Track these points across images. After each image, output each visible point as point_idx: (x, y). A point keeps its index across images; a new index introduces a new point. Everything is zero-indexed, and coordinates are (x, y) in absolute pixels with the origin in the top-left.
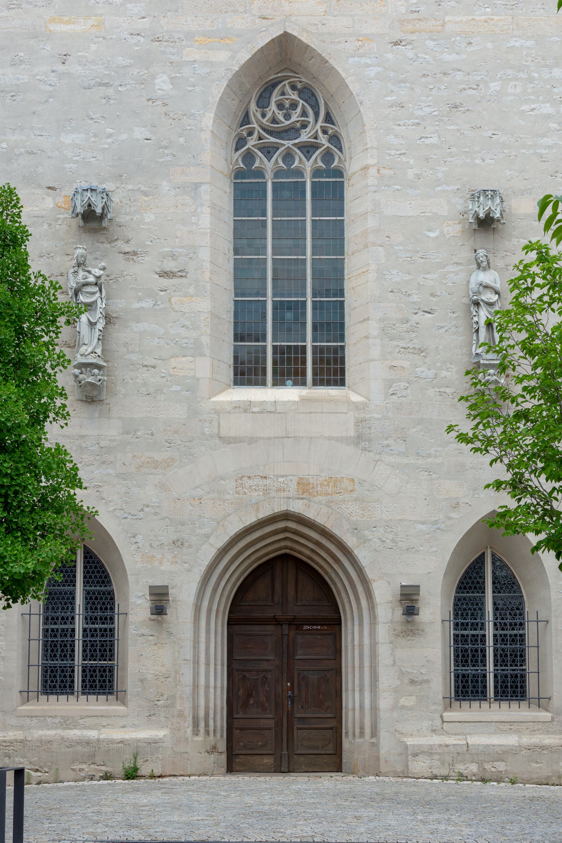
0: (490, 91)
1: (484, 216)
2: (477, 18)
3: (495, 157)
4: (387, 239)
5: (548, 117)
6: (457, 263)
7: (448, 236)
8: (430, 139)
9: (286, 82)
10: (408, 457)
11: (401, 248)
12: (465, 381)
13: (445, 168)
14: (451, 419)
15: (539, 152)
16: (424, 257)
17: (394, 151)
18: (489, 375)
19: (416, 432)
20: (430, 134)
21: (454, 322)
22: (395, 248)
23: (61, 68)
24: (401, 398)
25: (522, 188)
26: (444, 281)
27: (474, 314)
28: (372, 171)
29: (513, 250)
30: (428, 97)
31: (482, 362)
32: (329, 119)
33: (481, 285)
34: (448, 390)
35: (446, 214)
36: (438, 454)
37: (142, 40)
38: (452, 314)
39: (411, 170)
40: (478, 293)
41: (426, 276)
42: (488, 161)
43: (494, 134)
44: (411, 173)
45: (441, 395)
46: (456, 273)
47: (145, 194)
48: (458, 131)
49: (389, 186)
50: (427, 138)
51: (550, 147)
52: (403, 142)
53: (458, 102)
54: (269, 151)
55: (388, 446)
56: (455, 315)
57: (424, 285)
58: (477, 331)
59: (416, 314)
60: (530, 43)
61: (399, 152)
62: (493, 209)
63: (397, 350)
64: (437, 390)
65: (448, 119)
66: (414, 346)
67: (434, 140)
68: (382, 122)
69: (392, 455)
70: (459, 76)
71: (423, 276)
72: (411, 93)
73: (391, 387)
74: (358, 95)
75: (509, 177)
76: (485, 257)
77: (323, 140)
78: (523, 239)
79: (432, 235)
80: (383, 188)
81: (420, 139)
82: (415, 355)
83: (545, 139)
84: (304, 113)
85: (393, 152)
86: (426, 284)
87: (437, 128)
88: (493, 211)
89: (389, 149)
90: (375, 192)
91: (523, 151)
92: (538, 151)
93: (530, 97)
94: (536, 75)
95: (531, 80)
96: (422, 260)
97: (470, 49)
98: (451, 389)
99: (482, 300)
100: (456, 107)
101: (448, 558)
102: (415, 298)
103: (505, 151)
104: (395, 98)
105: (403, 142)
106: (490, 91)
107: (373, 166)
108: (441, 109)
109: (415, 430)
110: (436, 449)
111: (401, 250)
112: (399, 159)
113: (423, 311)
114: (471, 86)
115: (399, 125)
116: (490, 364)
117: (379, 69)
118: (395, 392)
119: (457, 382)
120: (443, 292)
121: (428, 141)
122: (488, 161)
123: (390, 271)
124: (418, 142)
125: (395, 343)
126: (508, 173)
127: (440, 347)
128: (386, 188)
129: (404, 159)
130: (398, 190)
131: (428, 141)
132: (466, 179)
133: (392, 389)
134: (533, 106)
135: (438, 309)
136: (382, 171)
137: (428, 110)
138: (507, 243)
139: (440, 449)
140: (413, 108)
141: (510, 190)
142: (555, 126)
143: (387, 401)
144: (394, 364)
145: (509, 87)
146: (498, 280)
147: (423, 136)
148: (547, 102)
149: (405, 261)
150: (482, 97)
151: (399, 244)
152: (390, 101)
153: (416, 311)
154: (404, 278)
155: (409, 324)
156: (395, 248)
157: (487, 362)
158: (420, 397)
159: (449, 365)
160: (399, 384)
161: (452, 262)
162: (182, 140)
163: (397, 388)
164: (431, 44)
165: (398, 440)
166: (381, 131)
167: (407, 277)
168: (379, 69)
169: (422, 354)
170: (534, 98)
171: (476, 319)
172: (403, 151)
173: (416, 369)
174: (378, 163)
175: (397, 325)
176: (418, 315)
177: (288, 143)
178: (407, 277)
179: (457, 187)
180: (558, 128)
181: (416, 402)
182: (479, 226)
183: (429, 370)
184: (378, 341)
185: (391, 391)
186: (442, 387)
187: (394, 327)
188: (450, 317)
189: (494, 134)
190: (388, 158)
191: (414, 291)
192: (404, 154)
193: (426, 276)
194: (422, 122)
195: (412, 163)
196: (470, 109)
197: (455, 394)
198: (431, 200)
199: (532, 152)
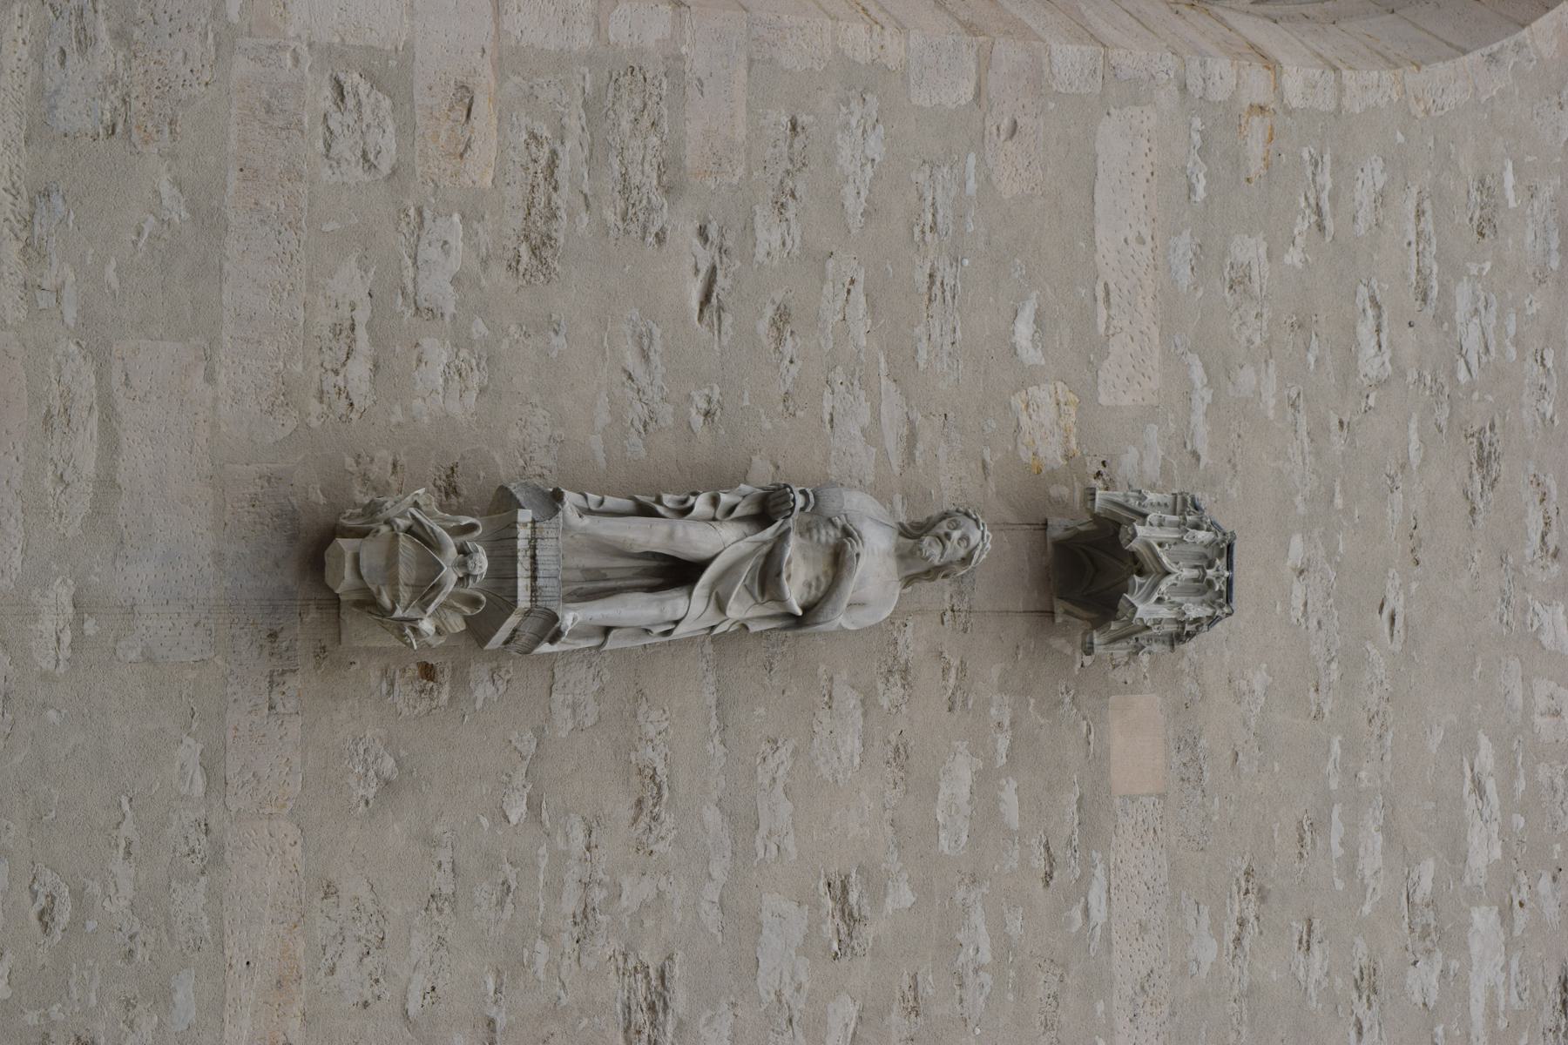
0: (1538, 606)
1: (1135, 545)
3: (1313, 624)
4: (1006, 124)
5: (1456, 853)
6: (912, 439)
7: (1017, 401)
8: (1373, 342)
10: (28, 140)
11: (972, 185)
12: (403, 460)
13: (1272, 402)
14: (222, 378)
15: (1335, 816)
16: (937, 289)
17: (1329, 186)
18: (463, 551)
19: (157, 193)
20: (1391, 343)
21: (666, 414)
22: (972, 160)
24: (320, 129)
25: (1203, 742)
26: (839, 376)
27: (726, 499)
28: (1257, 86)
29: (965, 703)
30: (1517, 342)
31: (525, 515)
33: (847, 533)
34: (359, 370)
35: (1104, 399)
36: (45, 300)
38: (703, 405)
39: (1262, 250)
40: (817, 517)
41: (858, 291)
42: (1298, 590)
43: (1393, 619)
44: (1249, 249)
45: (336, 331)
46: (872, 435)
48: (1403, 467)
49: (1204, 152)
50: (1378, 331)
51: (1350, 866)
52: (1361, 228)
53: (1501, 468)
55: (85, 41)
56: (698, 420)
57: (823, 280)
58: (645, 511)
59: (703, 233)
61: (1326, 207)
62: (1163, 587)
63: (544, 131)
64: (362, 316)
65: (1444, 424)
66: (562, 213)
67: (1371, 363)
68: (1431, 144)
69: (39, 59)
71: (861, 278)
72: (1529, 271)
73: (376, 83)
74: (1520, 46)
75: (1244, 688)
76: (962, 552)
78: (1011, 748)
79: (1024, 330)
80: (1197, 123)
81: (1373, 299)
82: (521, 214)
83: (1380, 838)
85: (1326, 179)
86: (828, 289)
87: (1412, 376)
88: (1155, 586)
89: (1337, 161)
90: (1183, 88)
91: (1336, 749)
92: (1337, 810)
93: (1522, 772)
96: (921, 278)
98: (365, 387)
99: (782, 537)
100: (1483, 461)
102: (768, 236)
103: (1334, 666)
104: (1512, 204)
105: (1361, 228)
106: (1538, 606)
107: (1278, 88)
108: (1476, 396)
109: (166, 188)
110: (69, 293)
111: (963, 184)
112: (1303, 204)
113: (713, 271)
114: (1554, 523)
115: (1420, 214)
116: (514, 558)
118: (350, 102)
119: (398, 416)
120: (794, 369)
121: (1365, 330)
123: (880, 128)
124: (1363, 292)
125: (574, 123)
126: (1259, 679)
127: (559, 342)
128: (1196, 137)
129: (1302, 225)
130: (1191, 189)
131: (1365, 330)
132: (1233, 493)
133: (364, 88)
134: (1490, 786)
135: (725, 340)
136: (1257, 127)
137: (1472, 343)
138: (995, 672)
139: (71, 314)
140: (1479, 277)
141: (1194, 688)
142: (1426, 884)
143: (307, 60)
144: (482, 106)
145: (1553, 684)
146: (863, 619)
147: (1385, 316)
148: (1506, 848)
149: (921, 198)
150: (1517, 569)
151: (988, 178)
152: (1502, 182)
153: (713, 232)
154: (849, 190)
155: (658, 199)
156: (972, 160)
157: (522, 544)
158: (327, 228)
159: (475, 380)
160: (391, 129)
161: (917, 416)
163: (367, 111)
165: (114, 97)
166: (1400, 138)
167: (854, 205)
169: (524, 250)
170: (1519, 794)
171: (701, 504)
172: (1329, 224)
173: (456, 218)
174: (1289, 112)
175: (654, 140)
176: (696, 242)
178: (854, 205)
179: (1203, 450)
180: (1417, 898)
181: (304, 203)
182: (1062, 546)
183: (456, 280)
184: (583, 39)
185: (352, 80)
186: (375, 341)
187: (646, 122)
188: (689, 398)
189: (1393, 619)
190: (1306, 156)
191: (796, 231)
192: (1321, 227)
193: (858, 291)
194: (1429, 311)
195: (1288, 259)
196: (1479, 518)
197: (343, 402)
198: (1155, 331)
199: (1334, 785)
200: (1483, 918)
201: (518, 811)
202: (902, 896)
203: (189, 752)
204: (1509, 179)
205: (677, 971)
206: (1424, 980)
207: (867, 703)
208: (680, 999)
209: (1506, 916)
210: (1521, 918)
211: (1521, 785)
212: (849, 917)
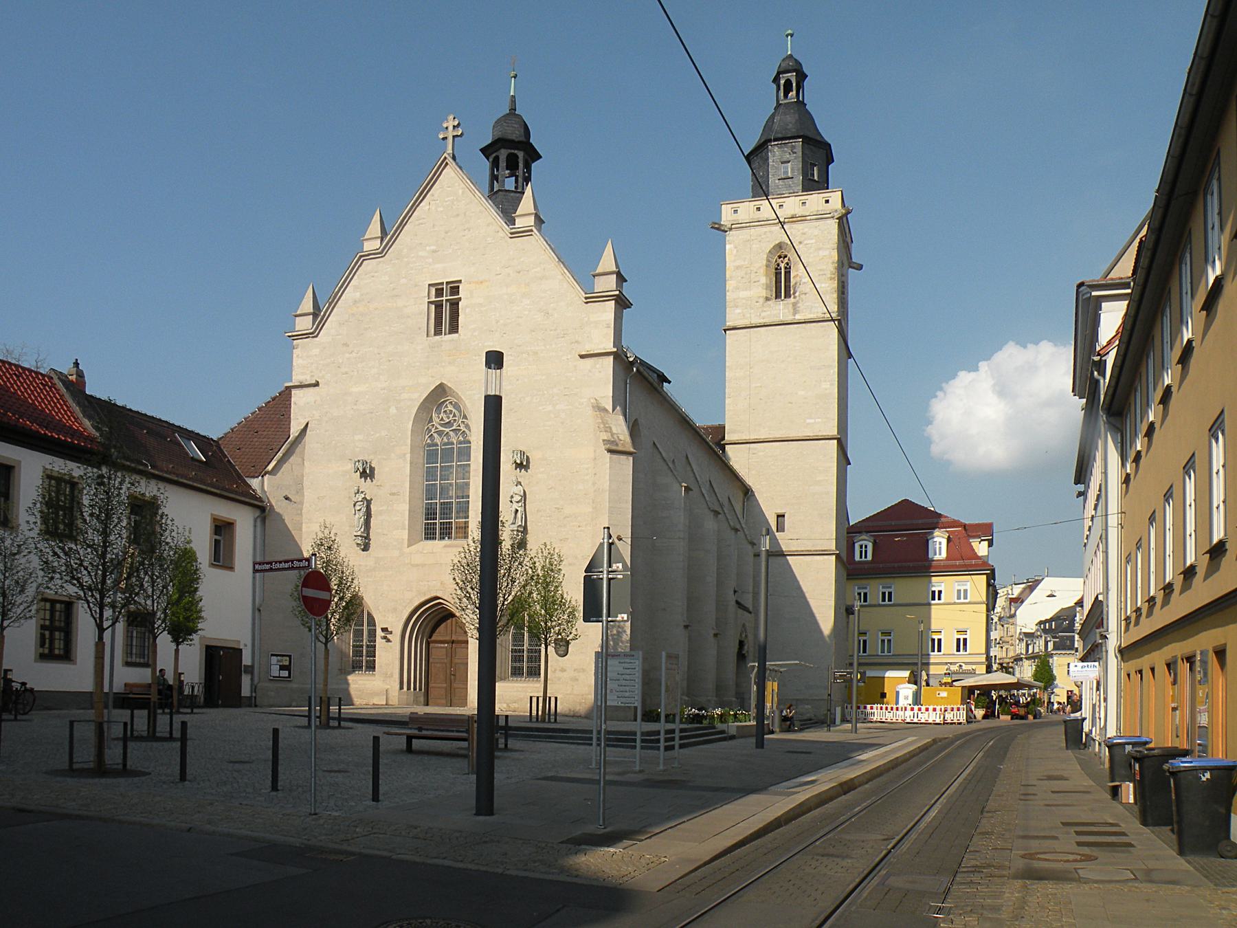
2: (522, 368)
9: (447, 402)
23: (355, 407)
32: (465, 417)
47: (385, 459)
54: (440, 433)
77: (462, 428)
84: (454, 416)
94: (546, 392)
134: (544, 407)
162: (400, 434)
177: (447, 430)
201: (540, 524)
208: (558, 506)
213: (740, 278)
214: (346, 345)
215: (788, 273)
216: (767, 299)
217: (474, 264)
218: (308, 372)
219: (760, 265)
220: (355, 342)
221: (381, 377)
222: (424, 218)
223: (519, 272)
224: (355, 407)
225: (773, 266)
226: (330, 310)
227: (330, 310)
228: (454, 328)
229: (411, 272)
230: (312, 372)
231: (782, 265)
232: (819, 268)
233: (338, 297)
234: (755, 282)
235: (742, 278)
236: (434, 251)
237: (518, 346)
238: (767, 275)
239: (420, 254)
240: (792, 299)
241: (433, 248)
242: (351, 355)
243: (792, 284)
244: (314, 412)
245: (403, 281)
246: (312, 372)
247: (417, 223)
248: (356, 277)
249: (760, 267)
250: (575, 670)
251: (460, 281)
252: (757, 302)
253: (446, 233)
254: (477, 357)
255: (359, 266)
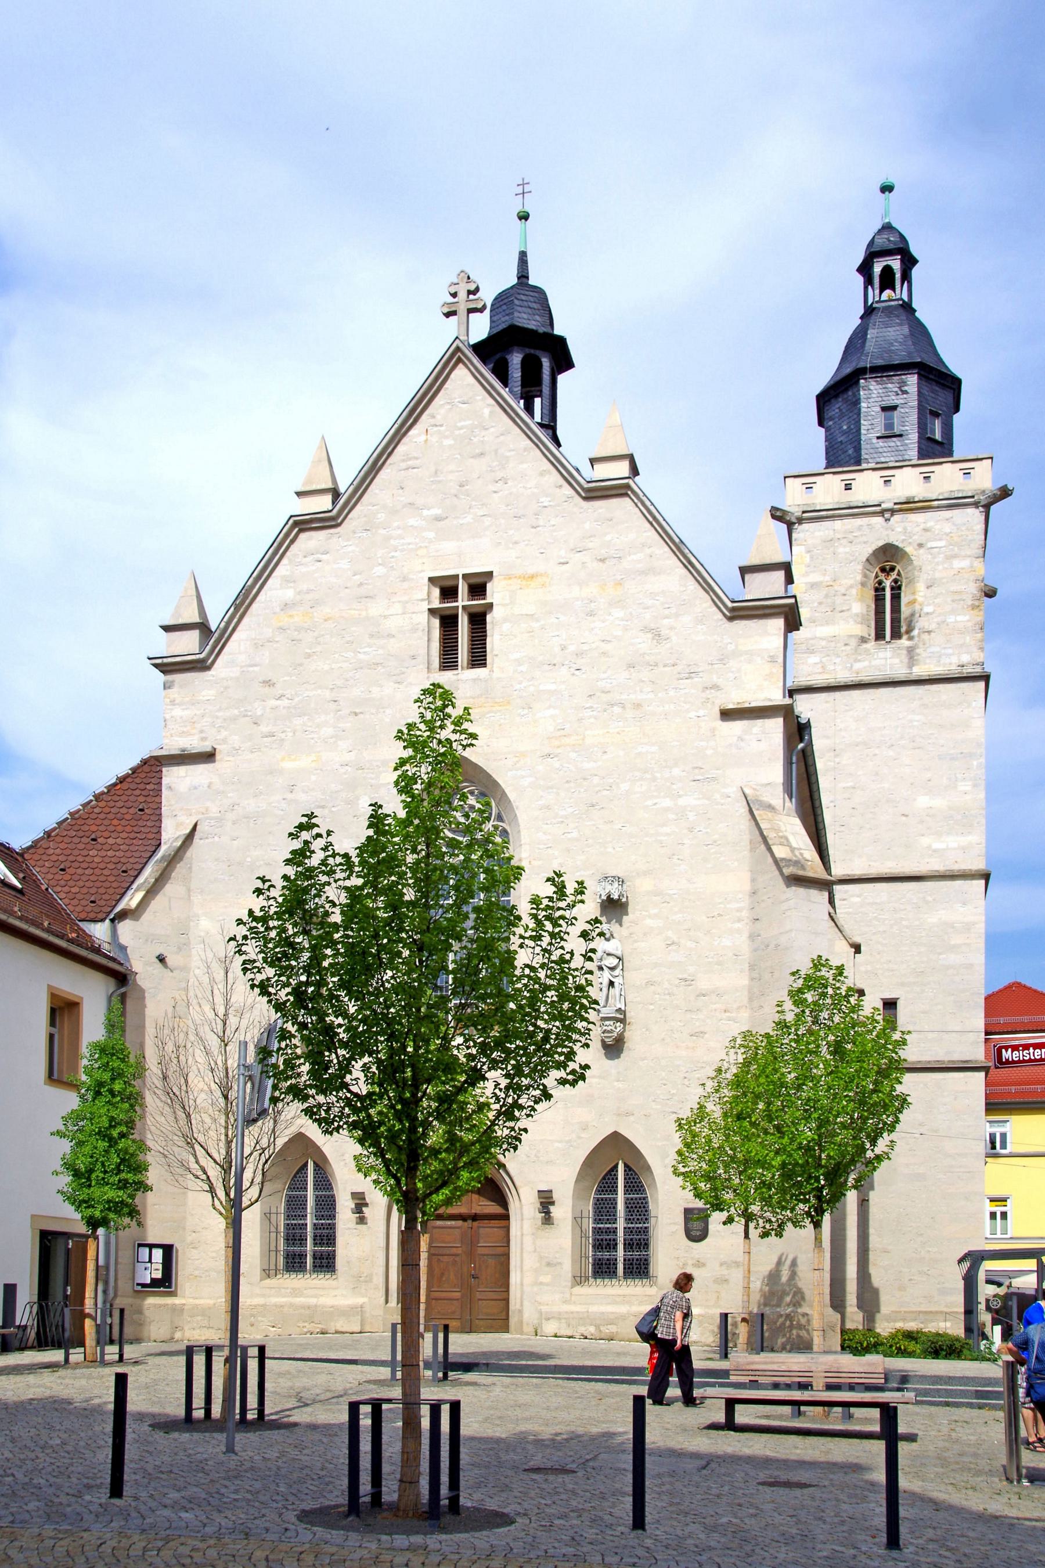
5: (667, 810)
37: (349, 769)
51: (668, 834)
60: (654, 749)
67: (575, 834)
70: (596, 780)
85: (541, 847)
95: (654, 779)
97: (605, 757)
100: (593, 806)
101: (578, 1169)
117: (532, 779)
122: (618, 849)
129: (550, 851)
131: (569, 836)
134: (655, 801)
136: (533, 862)
137: (570, 810)
164: (573, 755)
168: (532, 779)
200: (681, 802)
201: (652, 1007)
202: (670, 933)
203: (641, 1063)
204: (540, 802)
205: (680, 976)
206: (691, 816)
207: (636, 941)
208: (685, 976)
209: (680, 796)
210: (681, 793)
211: (655, 794)
212: (673, 943)
213: (816, 604)
214: (268, 683)
215: (896, 598)
216: (863, 640)
217: (516, 543)
218: (194, 731)
219: (852, 582)
220: (286, 678)
221: (340, 743)
222: (417, 458)
223: (602, 560)
224: (289, 796)
225: (872, 583)
226: (236, 620)
227: (236, 620)
228: (478, 659)
229: (393, 554)
230: (202, 732)
231: (888, 584)
232: (952, 589)
233: (251, 596)
234: (842, 611)
235: (820, 603)
236: (438, 519)
237: (603, 692)
238: (861, 599)
239: (412, 522)
240: (904, 642)
241: (437, 511)
242: (279, 702)
243: (903, 616)
244: (208, 804)
245: (380, 570)
246: (202, 732)
247: (403, 465)
248: (284, 561)
249: (851, 587)
250: (721, 1265)
251: (490, 575)
252: (846, 645)
253: (461, 486)
254: (526, 711)
255: (292, 542)
